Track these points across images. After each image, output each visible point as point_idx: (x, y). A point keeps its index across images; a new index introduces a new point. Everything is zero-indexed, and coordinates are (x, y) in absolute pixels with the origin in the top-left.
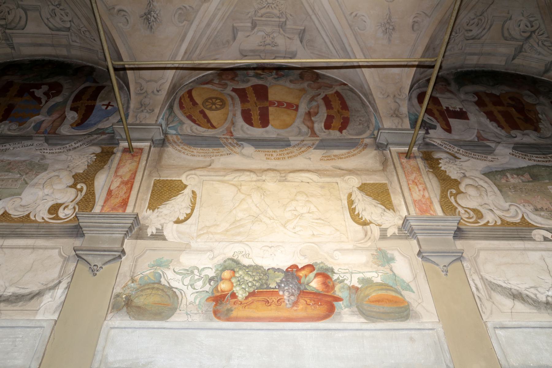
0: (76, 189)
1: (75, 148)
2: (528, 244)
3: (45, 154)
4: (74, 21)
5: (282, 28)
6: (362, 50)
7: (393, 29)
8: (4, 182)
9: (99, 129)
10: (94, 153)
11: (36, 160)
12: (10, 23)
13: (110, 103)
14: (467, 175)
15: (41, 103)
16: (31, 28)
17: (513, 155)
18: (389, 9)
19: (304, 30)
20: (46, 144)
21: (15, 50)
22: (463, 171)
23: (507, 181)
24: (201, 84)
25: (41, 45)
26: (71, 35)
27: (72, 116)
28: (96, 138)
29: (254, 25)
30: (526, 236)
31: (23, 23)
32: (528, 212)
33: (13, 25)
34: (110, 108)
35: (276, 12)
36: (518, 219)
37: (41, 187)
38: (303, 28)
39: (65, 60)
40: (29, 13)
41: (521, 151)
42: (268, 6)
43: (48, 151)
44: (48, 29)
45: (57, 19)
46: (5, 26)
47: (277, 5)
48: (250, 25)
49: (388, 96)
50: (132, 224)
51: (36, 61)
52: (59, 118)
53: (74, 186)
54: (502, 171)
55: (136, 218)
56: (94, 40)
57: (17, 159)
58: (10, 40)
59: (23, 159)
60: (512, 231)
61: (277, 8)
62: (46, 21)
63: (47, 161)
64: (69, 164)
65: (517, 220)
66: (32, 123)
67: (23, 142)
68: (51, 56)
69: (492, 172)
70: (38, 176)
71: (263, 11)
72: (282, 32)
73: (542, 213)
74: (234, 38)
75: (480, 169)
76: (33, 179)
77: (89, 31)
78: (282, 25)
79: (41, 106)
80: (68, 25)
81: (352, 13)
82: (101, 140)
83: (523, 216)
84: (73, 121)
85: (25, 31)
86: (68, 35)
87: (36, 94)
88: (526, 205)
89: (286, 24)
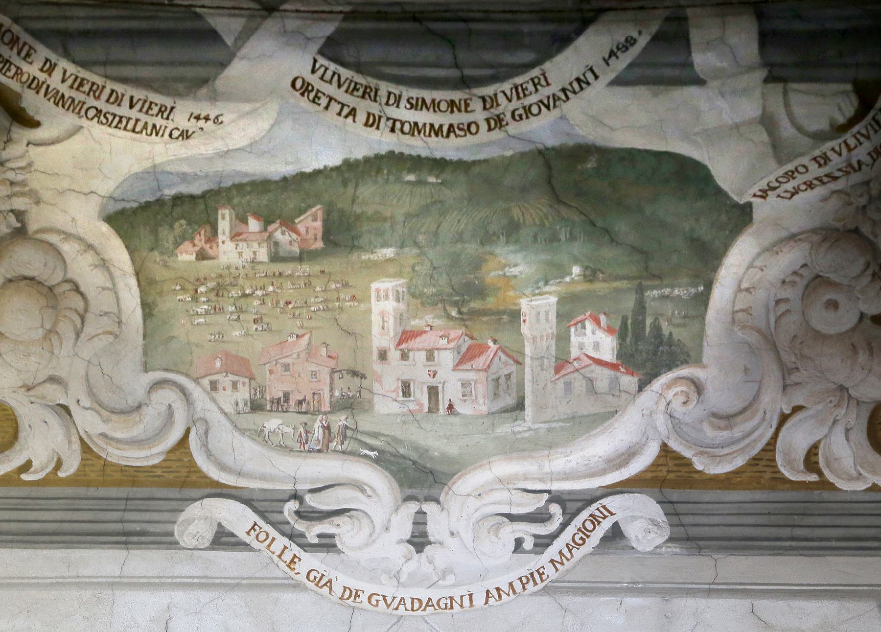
2: (143, 562)
14: (32, 227)
17: (306, 89)
22: (19, 203)
23: (202, 256)
30: (151, 528)
32: (215, 416)
36: (155, 450)
41: (358, 68)
54: (204, 196)
60: (104, 504)
65: (150, 457)
69: (160, 202)
73: (273, 423)
75: (106, 187)
83: (184, 440)
88: (225, 380)
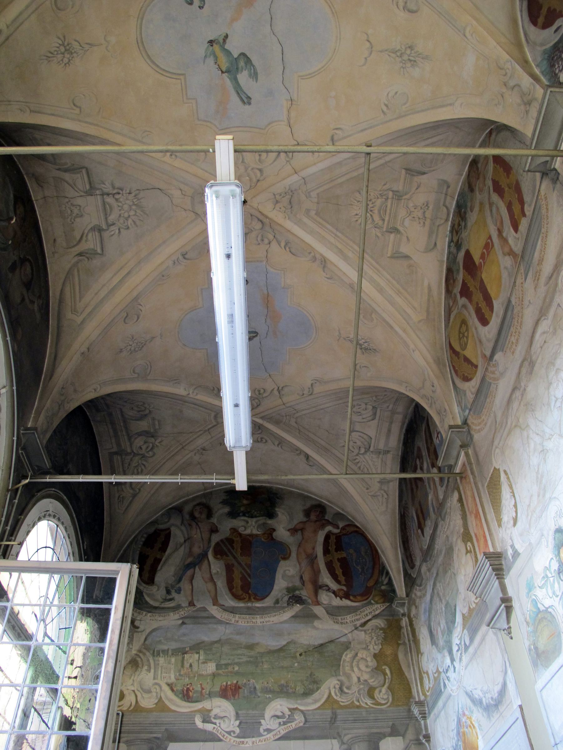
5: (402, 196)
6: (434, 108)
7: (411, 48)
12: (365, 445)
16: (372, 432)
18: (381, 52)
19: (407, 169)
24: (449, 323)
29: (395, 230)
31: (365, 436)
33: (366, 443)
35: (379, 202)
38: (403, 172)
42: (371, 211)
47: (370, 200)
48: (392, 236)
49: (502, 97)
50: (491, 565)
55: (486, 558)
61: (373, 201)
62: (364, 420)
71: (376, 218)
72: (407, 197)
74: (407, 257)
78: (398, 196)
81: (383, 111)
85: (373, 438)
89: (398, 191)
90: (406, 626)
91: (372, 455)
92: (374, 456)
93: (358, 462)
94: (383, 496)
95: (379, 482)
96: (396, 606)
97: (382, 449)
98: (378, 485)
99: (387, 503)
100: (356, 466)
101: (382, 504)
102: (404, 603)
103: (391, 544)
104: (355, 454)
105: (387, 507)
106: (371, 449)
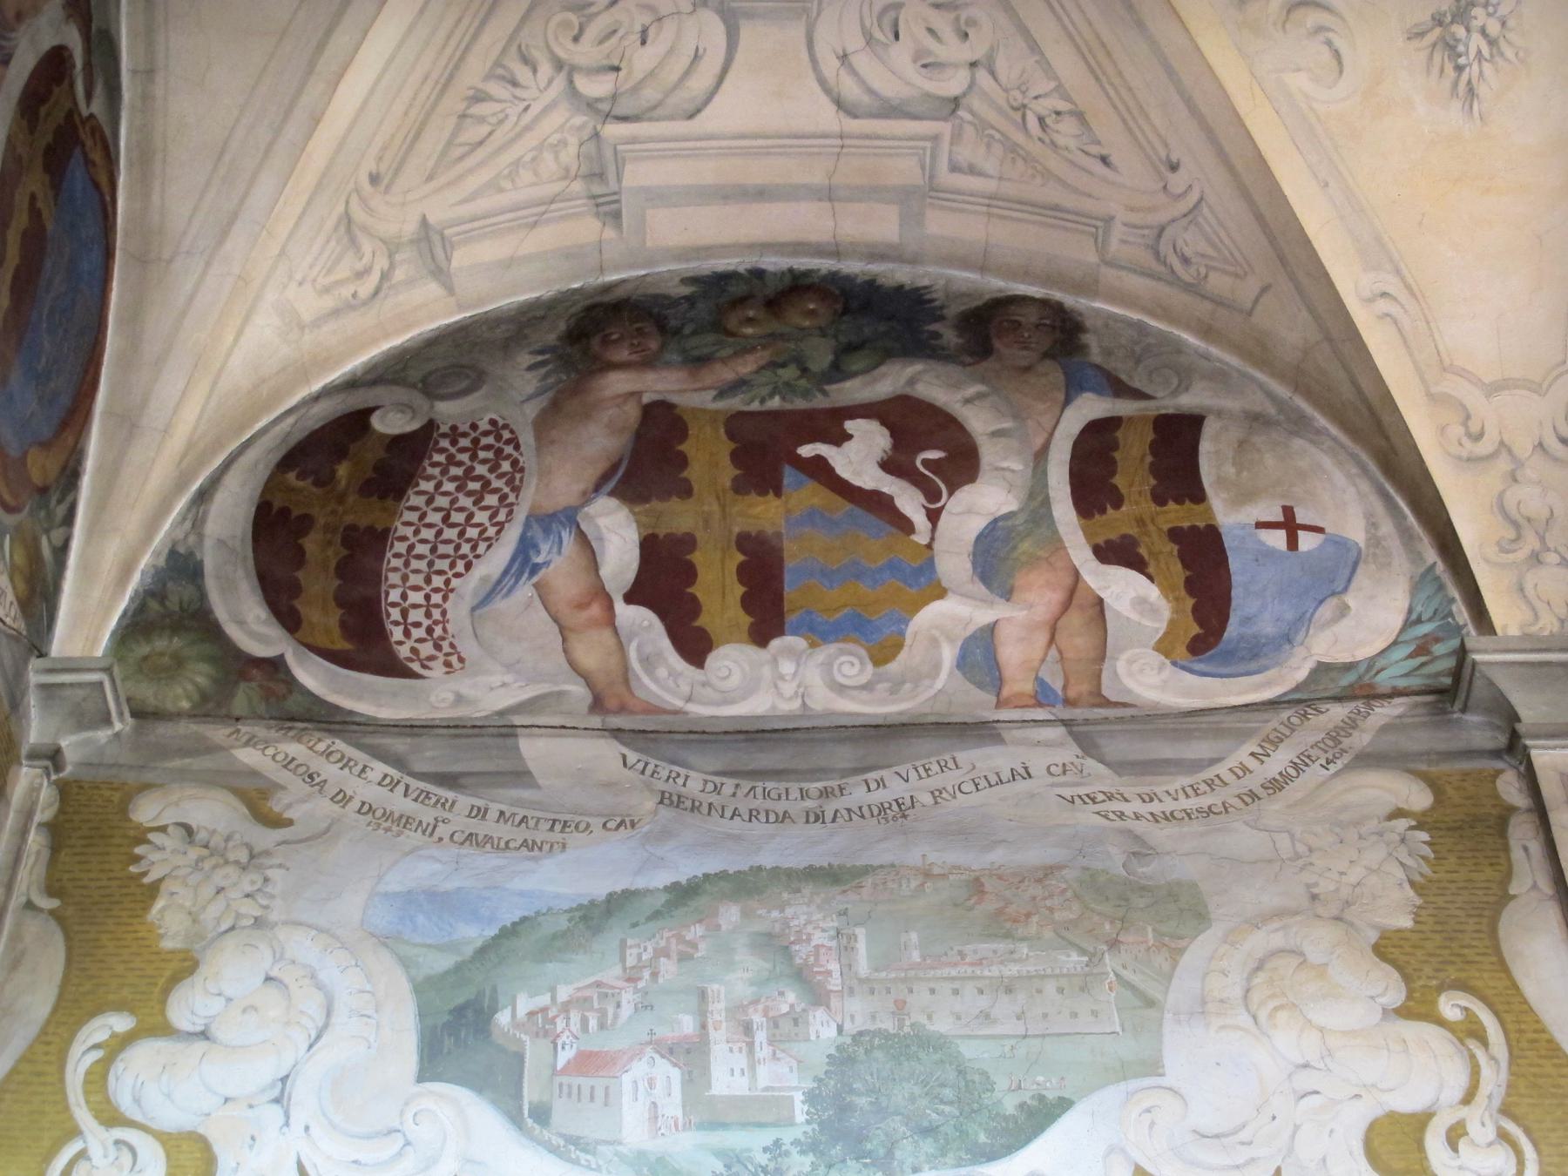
0: (1441, 1022)
1: (1275, 785)
3: (1140, 827)
4: (1001, 65)
8: (1021, 997)
9: (1322, 669)
10: (1398, 813)
11: (1114, 859)
12: (636, 89)
13: (1288, 511)
15: (906, 526)
16: (737, 109)
20: (1091, 764)
21: (619, 226)
25: (762, 194)
26: (956, 138)
27: (1135, 600)
28: (1351, 725)
33: (650, 94)
34: (1307, 541)
37: (1244, 1019)
39: (875, 268)
40: (747, 32)
43: (1136, 806)
44: (831, 108)
45: (901, 54)
46: (605, 107)
51: (722, 280)
52: (1067, 605)
53: (1417, 1008)
56: (1104, 160)
57: (998, 856)
58: (611, 176)
59: (1034, 855)
62: (830, 66)
63: (1185, 869)
64: (1308, 877)
66: (934, 643)
67: (961, 756)
68: (798, 248)
70: (1186, 959)
76: (1170, 978)
77: (1080, 116)
79: (921, 538)
80: (953, 84)
82: (1385, 729)
84: (1157, 626)
86: (936, 138)
87: (843, 471)
90: (28, 814)
91: (573, 141)
92: (569, 155)
93: (515, 84)
94: (360, 275)
95: (424, 222)
96: (44, 687)
97: (625, 183)
98: (411, 228)
99: (336, 313)
100: (488, 77)
101: (326, 290)
102: (107, 721)
103: (190, 445)
104: (565, 50)
105: (317, 323)
106: (613, 130)
